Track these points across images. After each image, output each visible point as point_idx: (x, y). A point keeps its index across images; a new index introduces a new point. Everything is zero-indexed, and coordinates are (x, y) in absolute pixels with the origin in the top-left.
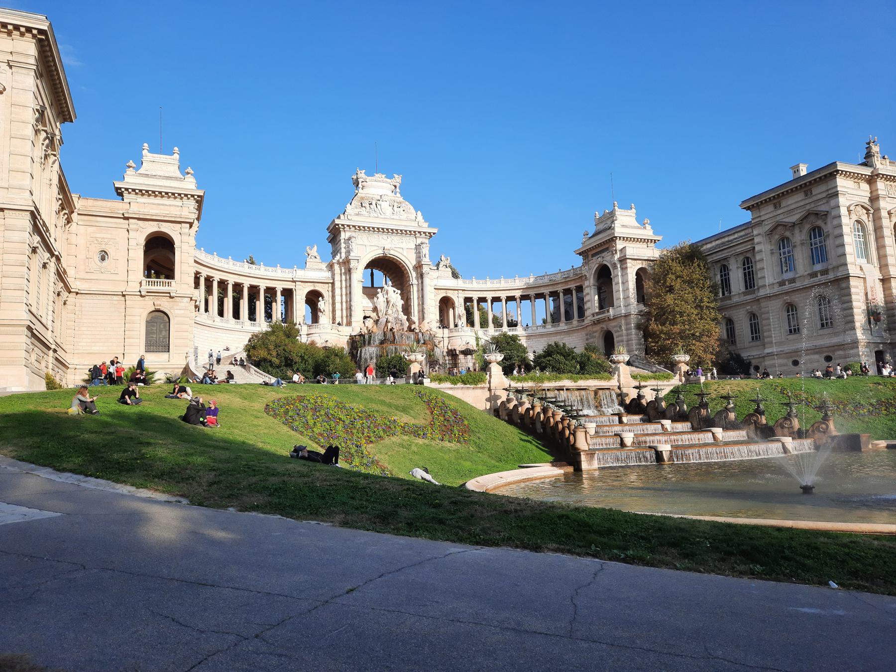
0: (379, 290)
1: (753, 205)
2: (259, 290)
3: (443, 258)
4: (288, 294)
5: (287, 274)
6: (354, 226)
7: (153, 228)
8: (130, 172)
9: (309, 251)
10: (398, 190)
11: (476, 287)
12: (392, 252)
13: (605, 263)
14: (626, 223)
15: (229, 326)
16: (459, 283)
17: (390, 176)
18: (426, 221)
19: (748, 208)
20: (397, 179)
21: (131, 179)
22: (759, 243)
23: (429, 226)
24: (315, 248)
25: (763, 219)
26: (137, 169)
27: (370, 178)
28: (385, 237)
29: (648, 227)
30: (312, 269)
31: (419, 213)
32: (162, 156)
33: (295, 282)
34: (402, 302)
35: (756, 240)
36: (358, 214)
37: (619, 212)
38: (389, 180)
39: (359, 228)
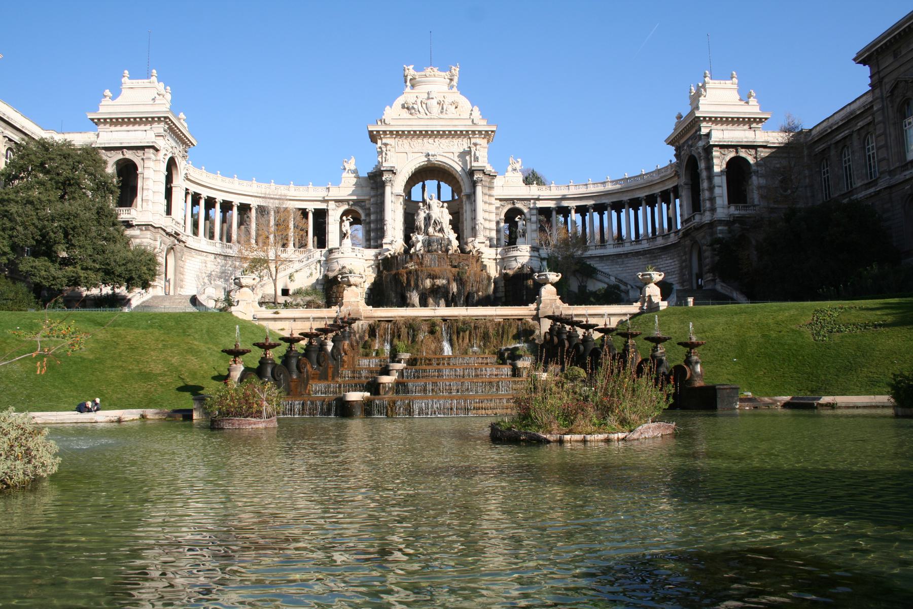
1: (867, 57)
4: (321, 216)
5: (320, 193)
6: (391, 132)
7: (119, 156)
9: (345, 164)
11: (547, 195)
12: (439, 158)
13: (693, 153)
14: (720, 98)
18: (483, 118)
24: (353, 161)
25: (882, 74)
26: (113, 98)
28: (431, 140)
31: (476, 109)
32: (140, 81)
34: (451, 217)
37: (711, 83)
38: (443, 74)
39: (399, 134)
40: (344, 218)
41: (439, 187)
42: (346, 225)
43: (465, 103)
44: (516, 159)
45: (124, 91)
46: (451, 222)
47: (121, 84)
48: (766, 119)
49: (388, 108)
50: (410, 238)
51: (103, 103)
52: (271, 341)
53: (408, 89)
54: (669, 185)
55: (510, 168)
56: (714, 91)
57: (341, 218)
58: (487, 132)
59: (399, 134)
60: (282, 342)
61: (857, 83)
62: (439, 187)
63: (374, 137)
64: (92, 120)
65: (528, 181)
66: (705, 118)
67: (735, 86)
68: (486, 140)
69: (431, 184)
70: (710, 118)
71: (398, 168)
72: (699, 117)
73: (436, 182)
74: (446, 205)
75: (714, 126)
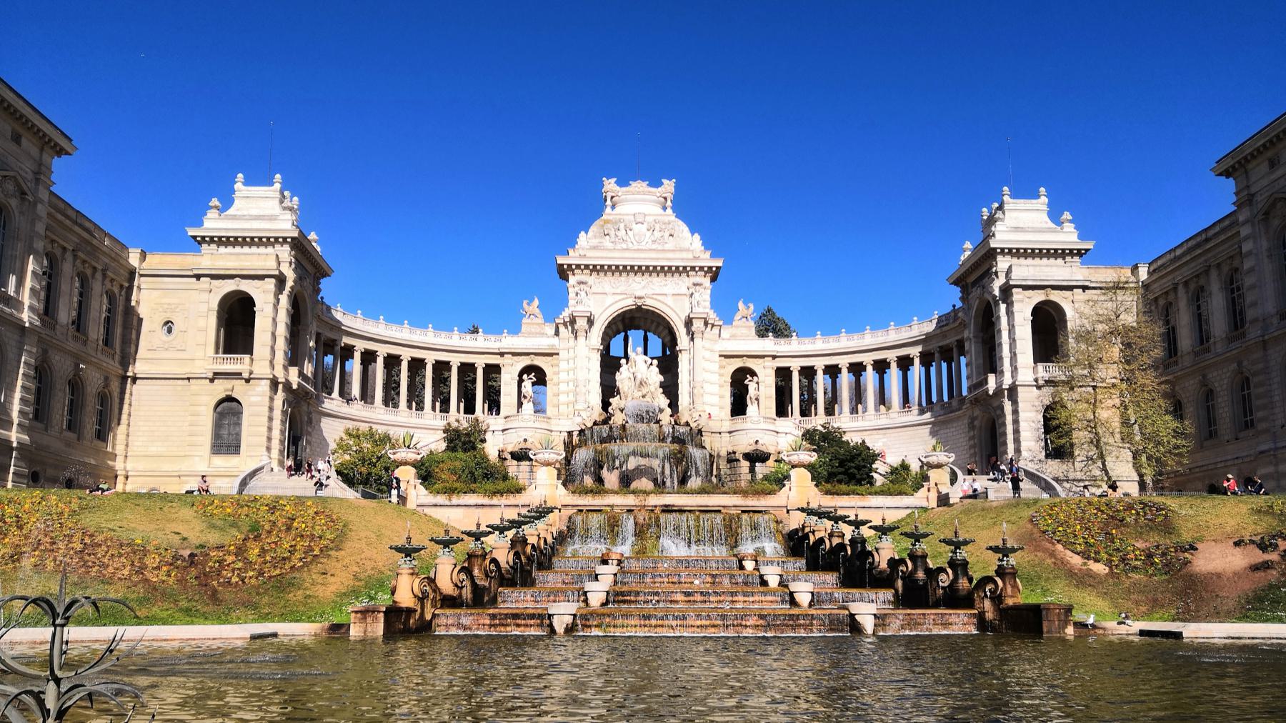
0: (623, 361)
1: (1234, 167)
2: (476, 369)
3: (741, 305)
4: (492, 371)
6: (587, 267)
8: (212, 214)
10: (669, 203)
12: (649, 302)
14: (1023, 220)
15: (380, 417)
16: (769, 344)
17: (656, 183)
19: (1227, 173)
20: (668, 186)
21: (213, 224)
22: (1246, 238)
23: (712, 256)
24: (536, 302)
27: (624, 189)
29: (1069, 227)
30: (530, 334)
31: (697, 236)
33: (502, 354)
34: (661, 378)
35: (1245, 231)
36: (595, 248)
39: (595, 269)
40: (525, 377)
41: (646, 339)
42: (527, 386)
43: (683, 228)
44: (746, 304)
45: (237, 203)
46: (662, 385)
47: (234, 192)
48: (1087, 250)
49: (583, 233)
50: (610, 404)
51: (209, 215)
52: (454, 534)
53: (608, 210)
54: (951, 340)
55: (738, 317)
56: (1015, 214)
57: (520, 375)
58: (710, 268)
59: (595, 269)
60: (465, 537)
61: (1219, 200)
62: (646, 339)
63: (563, 272)
64: (194, 237)
65: (762, 333)
66: (1003, 249)
67: (1045, 207)
68: (708, 279)
69: (635, 336)
70: (1010, 250)
71: (596, 313)
72: (995, 249)
73: (641, 333)
74: (655, 362)
75: (1015, 260)
